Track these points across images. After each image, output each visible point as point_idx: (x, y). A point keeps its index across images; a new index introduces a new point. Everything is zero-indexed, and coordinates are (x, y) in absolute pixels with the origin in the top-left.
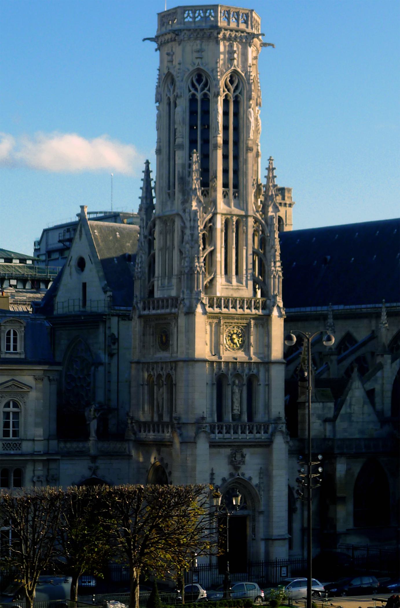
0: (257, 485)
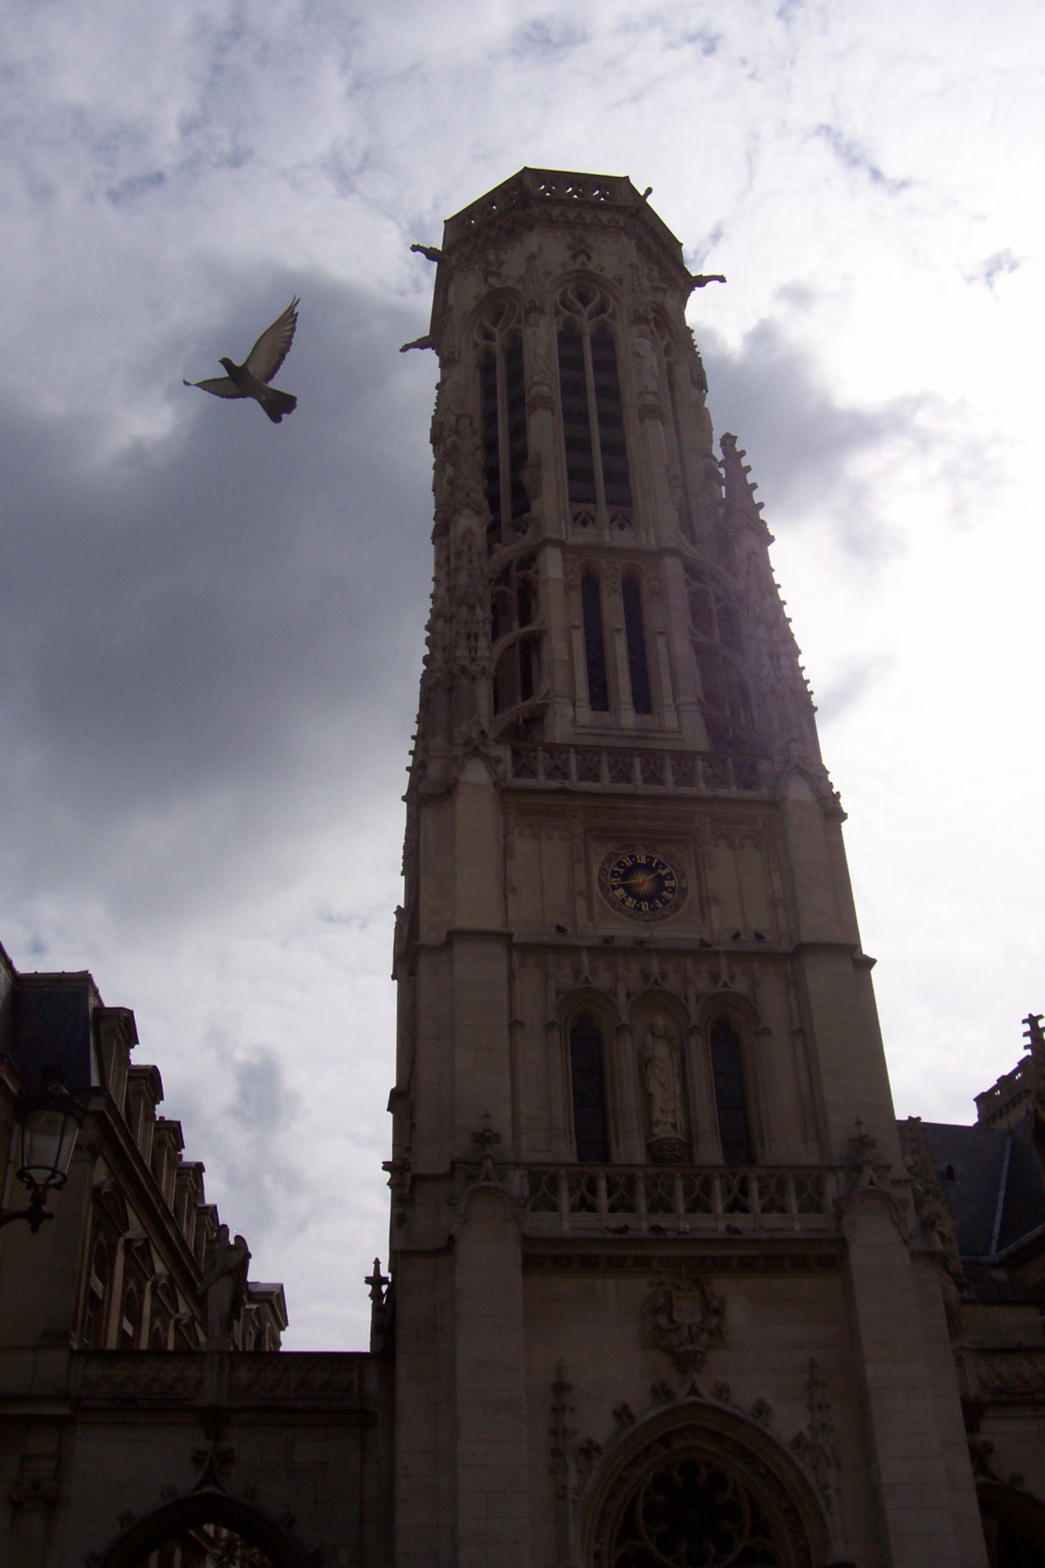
0: (798, 1442)
